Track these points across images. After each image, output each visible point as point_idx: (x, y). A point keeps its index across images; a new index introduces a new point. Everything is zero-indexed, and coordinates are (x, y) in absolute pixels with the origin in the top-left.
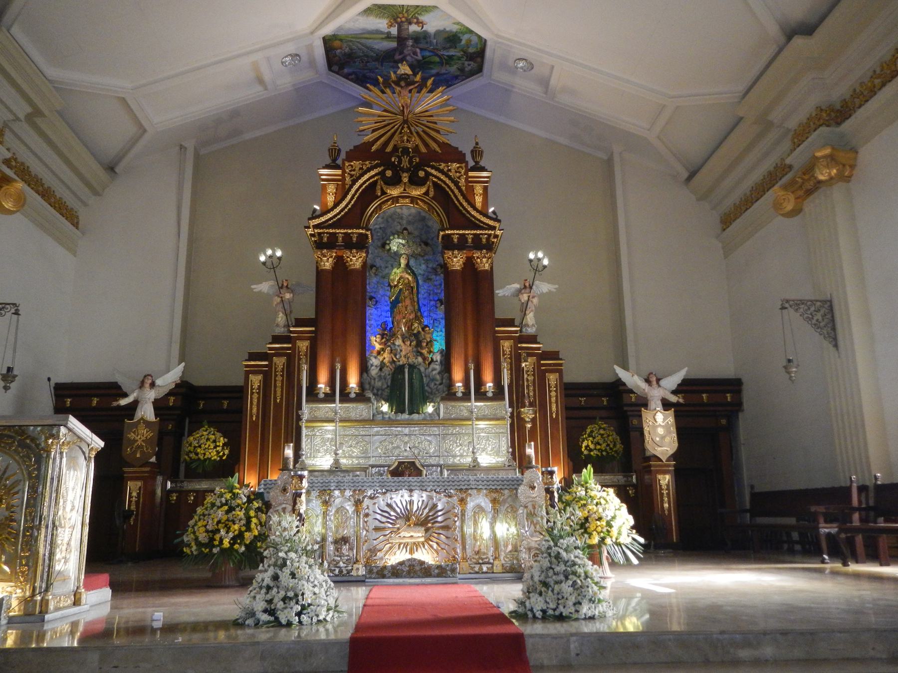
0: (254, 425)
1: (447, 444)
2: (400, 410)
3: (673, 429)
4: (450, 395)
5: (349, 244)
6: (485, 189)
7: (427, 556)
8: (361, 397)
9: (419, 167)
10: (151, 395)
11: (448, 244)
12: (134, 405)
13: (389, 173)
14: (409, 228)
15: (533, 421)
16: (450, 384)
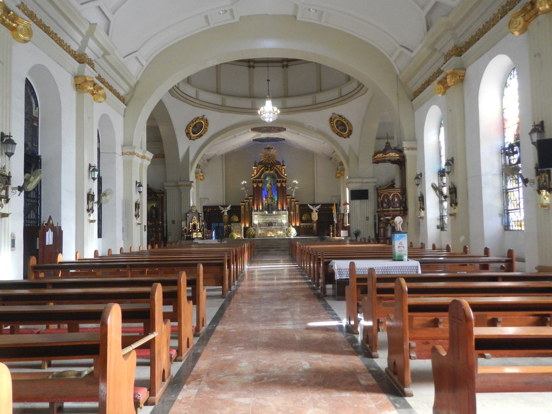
0: (243, 215)
1: (277, 219)
2: (269, 213)
3: (317, 216)
4: (278, 210)
5: (259, 182)
6: (285, 170)
7: (273, 235)
8: (262, 211)
9: (272, 167)
10: (226, 211)
11: (277, 182)
12: (224, 212)
13: (266, 168)
14: (271, 174)
15: (293, 214)
16: (278, 208)
